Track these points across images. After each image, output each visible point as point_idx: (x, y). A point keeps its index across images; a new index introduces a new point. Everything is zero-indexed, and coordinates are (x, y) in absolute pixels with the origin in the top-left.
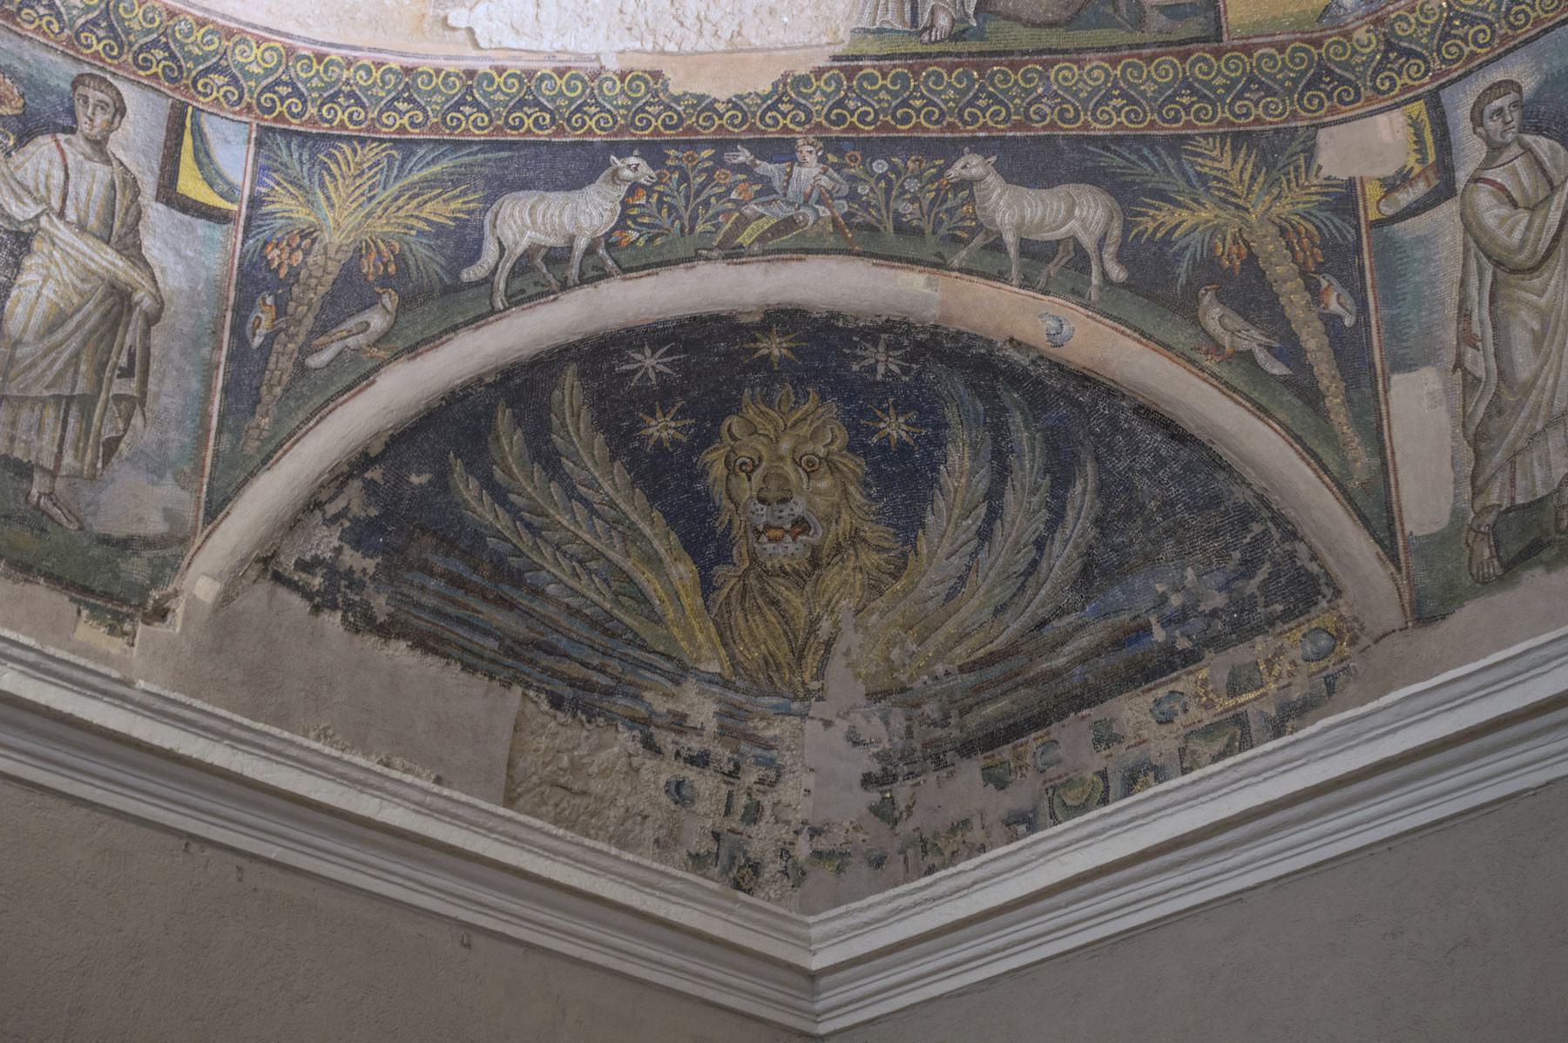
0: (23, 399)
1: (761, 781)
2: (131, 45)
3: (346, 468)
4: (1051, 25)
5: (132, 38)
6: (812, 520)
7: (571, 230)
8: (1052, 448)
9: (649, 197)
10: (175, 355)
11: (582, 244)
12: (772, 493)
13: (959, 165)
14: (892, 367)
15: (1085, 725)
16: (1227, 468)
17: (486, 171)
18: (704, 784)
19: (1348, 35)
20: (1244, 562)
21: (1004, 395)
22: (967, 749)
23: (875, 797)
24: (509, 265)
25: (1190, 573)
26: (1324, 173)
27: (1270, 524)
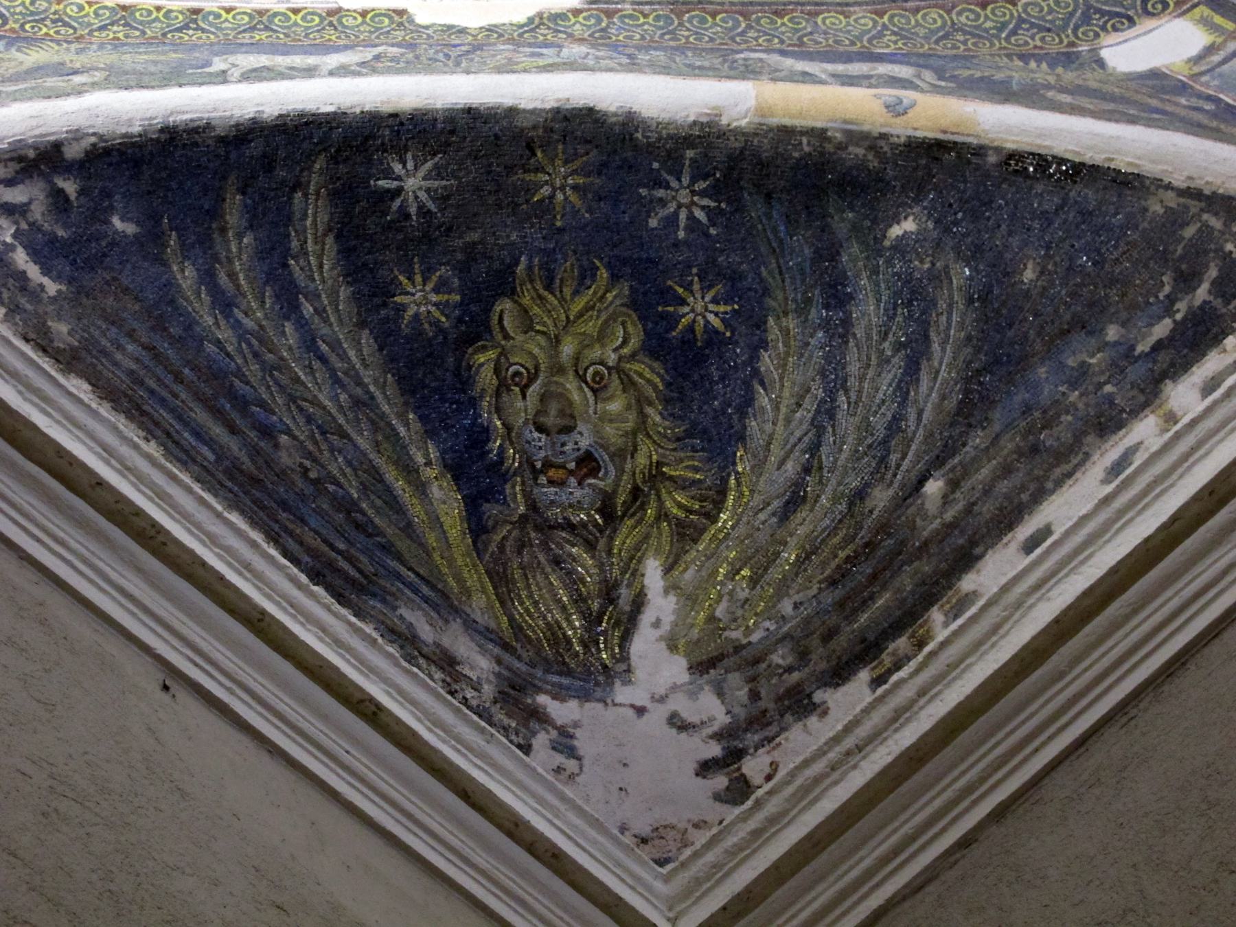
3: (31, 154)
6: (603, 456)
23: (720, 781)
27: (1205, 216)
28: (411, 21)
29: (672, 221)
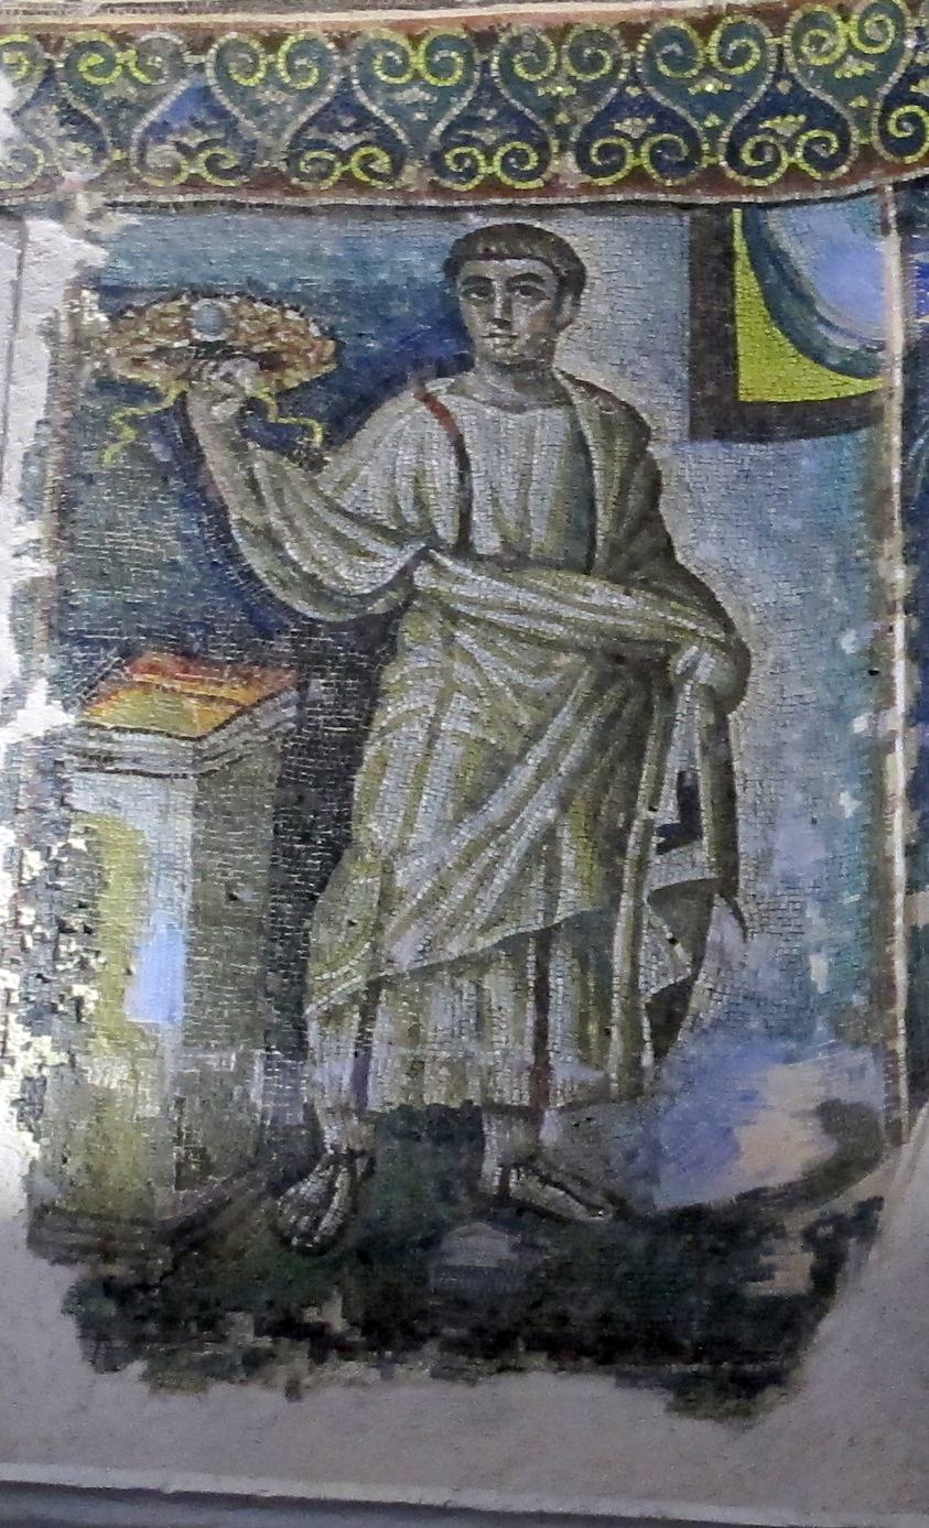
2: (562, 132)
5: (562, 118)
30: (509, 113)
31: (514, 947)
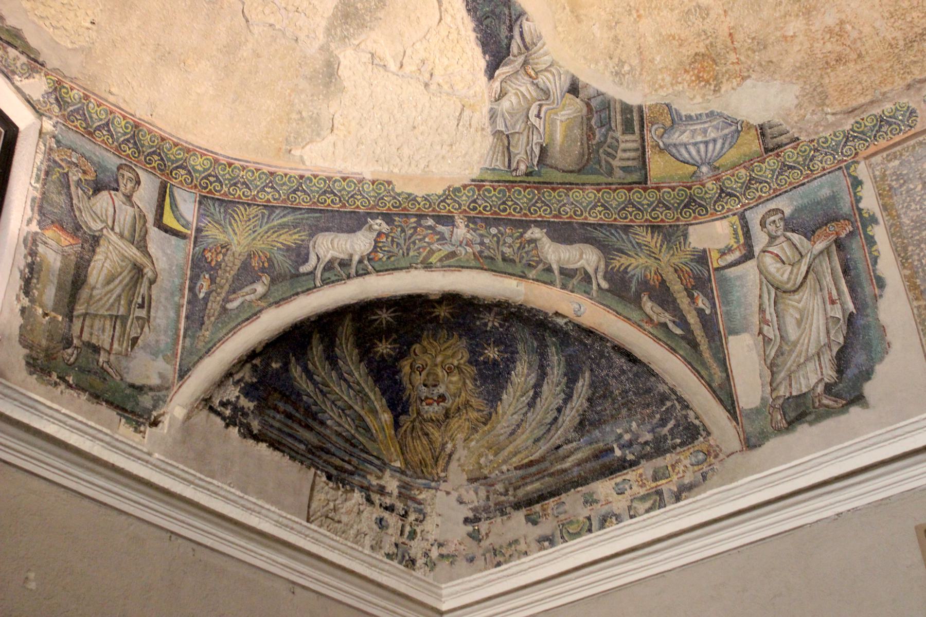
0: (96, 315)
1: (416, 520)
4: (571, 172)
6: (447, 395)
7: (351, 251)
8: (569, 364)
9: (387, 238)
10: (162, 300)
11: (356, 258)
12: (430, 382)
13: (529, 232)
14: (496, 324)
15: (579, 495)
16: (655, 375)
17: (309, 222)
18: (392, 520)
19: (703, 185)
20: (661, 419)
21: (548, 339)
22: (517, 506)
24: (322, 266)
25: (634, 424)
26: (692, 245)
28: (393, 189)
29: (486, 325)
30: (135, 142)
31: (111, 316)
